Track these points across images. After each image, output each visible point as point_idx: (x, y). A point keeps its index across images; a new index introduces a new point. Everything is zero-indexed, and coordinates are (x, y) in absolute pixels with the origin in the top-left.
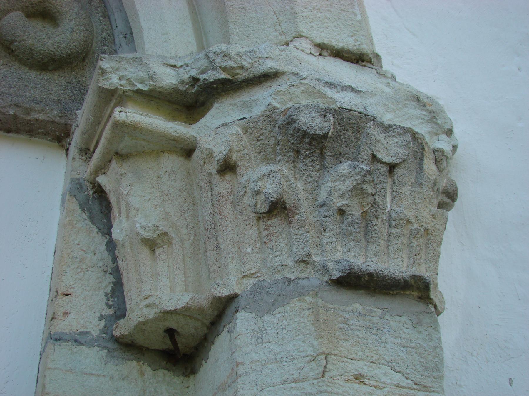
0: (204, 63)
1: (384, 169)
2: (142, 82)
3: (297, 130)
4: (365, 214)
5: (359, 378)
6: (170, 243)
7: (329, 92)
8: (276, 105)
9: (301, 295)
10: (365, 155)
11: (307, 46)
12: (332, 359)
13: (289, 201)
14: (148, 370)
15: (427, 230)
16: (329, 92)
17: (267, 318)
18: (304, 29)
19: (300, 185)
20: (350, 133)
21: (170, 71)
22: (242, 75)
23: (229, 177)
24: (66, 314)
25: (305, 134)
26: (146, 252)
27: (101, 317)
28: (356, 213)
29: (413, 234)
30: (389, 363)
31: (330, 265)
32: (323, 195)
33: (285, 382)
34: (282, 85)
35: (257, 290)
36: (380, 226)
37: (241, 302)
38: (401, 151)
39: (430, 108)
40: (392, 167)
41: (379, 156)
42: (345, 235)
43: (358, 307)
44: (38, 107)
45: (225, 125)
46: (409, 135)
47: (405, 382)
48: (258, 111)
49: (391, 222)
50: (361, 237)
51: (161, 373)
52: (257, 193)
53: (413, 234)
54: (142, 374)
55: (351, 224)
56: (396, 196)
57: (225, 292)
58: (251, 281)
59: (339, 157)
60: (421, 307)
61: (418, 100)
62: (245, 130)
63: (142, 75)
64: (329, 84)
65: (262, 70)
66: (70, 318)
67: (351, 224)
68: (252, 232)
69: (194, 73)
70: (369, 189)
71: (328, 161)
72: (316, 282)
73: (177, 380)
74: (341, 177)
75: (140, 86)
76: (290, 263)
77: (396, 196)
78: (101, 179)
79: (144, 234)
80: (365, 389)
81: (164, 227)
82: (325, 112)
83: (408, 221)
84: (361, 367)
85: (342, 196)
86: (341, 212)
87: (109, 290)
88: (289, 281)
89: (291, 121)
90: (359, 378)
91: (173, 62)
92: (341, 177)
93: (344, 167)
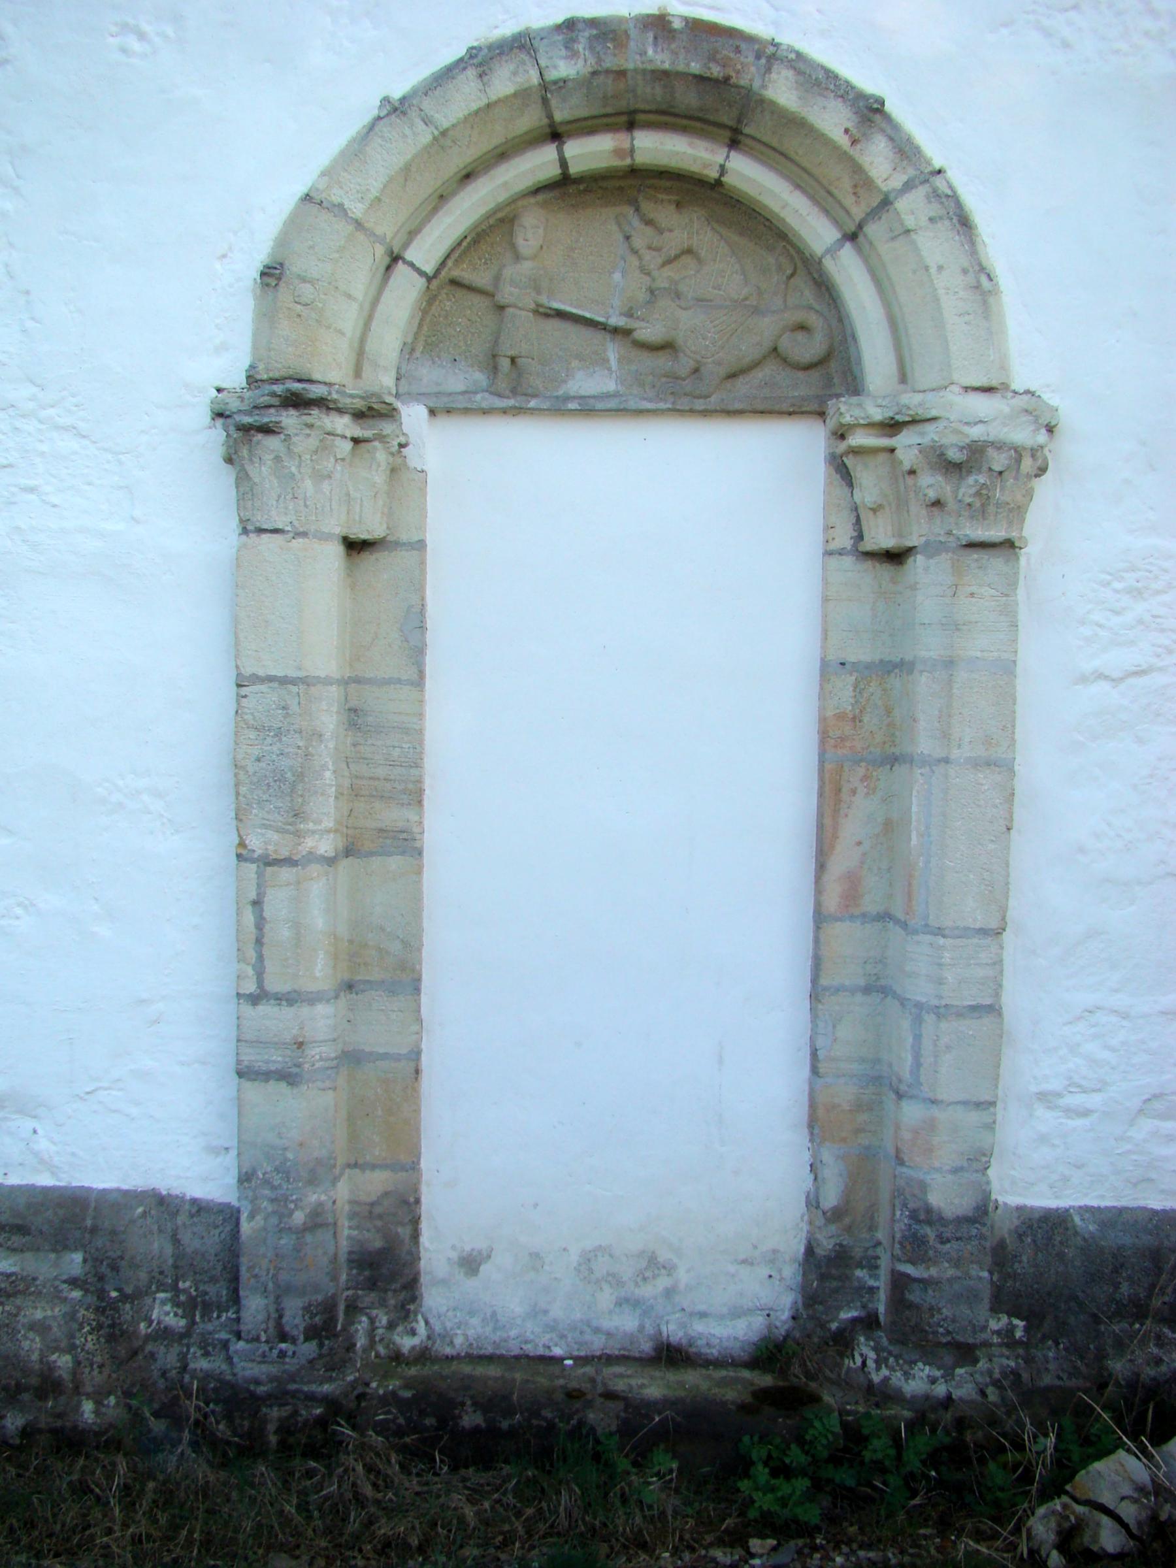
0: (895, 409)
1: (995, 474)
2: (863, 418)
3: (946, 460)
4: (983, 505)
5: (972, 595)
6: (884, 508)
7: (966, 429)
8: (937, 439)
9: (947, 551)
10: (984, 469)
11: (955, 389)
12: (959, 587)
13: (942, 501)
14: (878, 565)
15: (1019, 507)
16: (966, 429)
17: (931, 561)
18: (956, 377)
19: (948, 488)
20: (977, 455)
21: (879, 410)
22: (917, 418)
23: (912, 476)
24: (833, 539)
25: (950, 462)
26: (871, 513)
27: (851, 538)
28: (978, 505)
29: (1011, 510)
30: (989, 585)
31: (961, 537)
32: (960, 496)
33: (937, 596)
34: (941, 424)
35: (927, 544)
36: (991, 509)
37: (918, 549)
38: (1007, 462)
39: (1034, 414)
40: (1001, 473)
41: (993, 467)
42: (972, 517)
43: (975, 556)
44: (806, 404)
45: (909, 446)
46: (1013, 451)
47: (999, 594)
48: (926, 441)
49: (998, 505)
50: (980, 517)
51: (884, 565)
52: (925, 495)
53: (1011, 510)
54: (874, 567)
55: (975, 511)
56: (1002, 489)
57: (911, 544)
58: (923, 539)
59: (969, 472)
60: (1011, 550)
61: (1026, 411)
62: (920, 452)
63: (863, 415)
64: (967, 423)
65: (929, 416)
66: (836, 540)
67: (975, 511)
68: (924, 512)
69: (891, 414)
70: (984, 492)
71: (964, 474)
72: (954, 545)
73: (892, 568)
74: (971, 486)
75: (862, 422)
76: (942, 533)
77: (1002, 489)
78: (845, 459)
79: (871, 506)
80: (974, 600)
81: (879, 502)
82: (962, 449)
83: (1008, 504)
84: (974, 589)
85: (970, 496)
86: (969, 505)
87: (854, 521)
88: (940, 542)
89: (942, 454)
90: (972, 595)
91: (880, 401)
92: (971, 486)
93: (971, 480)
